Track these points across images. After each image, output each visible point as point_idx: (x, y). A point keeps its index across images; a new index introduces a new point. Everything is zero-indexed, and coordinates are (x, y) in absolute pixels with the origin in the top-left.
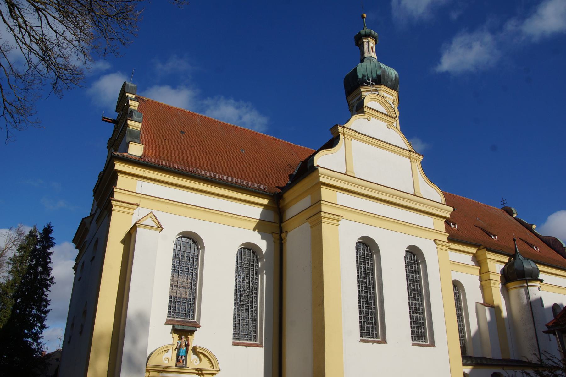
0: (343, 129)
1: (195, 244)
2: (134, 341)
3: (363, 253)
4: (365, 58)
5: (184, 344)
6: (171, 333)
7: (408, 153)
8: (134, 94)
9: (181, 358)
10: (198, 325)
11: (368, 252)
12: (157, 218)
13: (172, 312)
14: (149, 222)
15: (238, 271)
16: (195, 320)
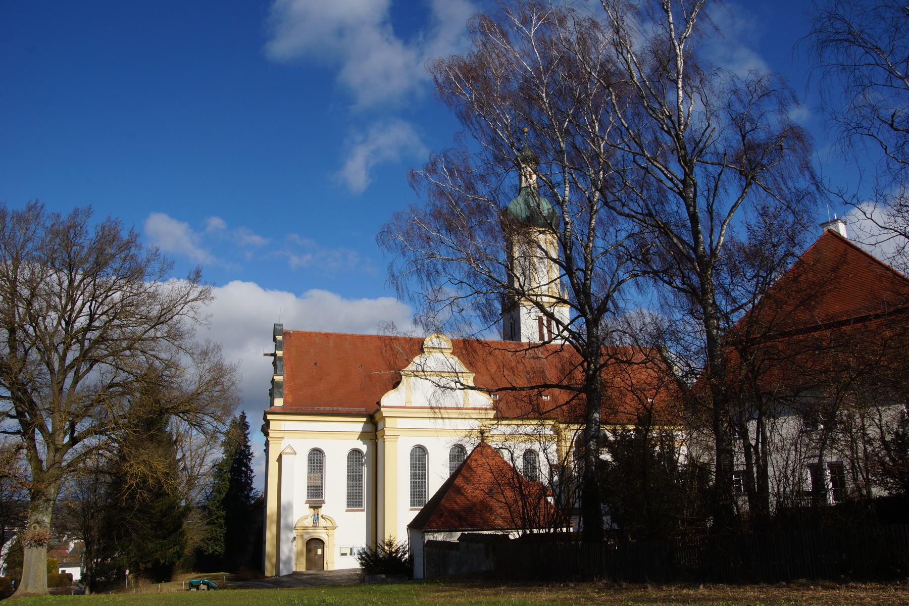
2: (286, 517)
13: (310, 495)
14: (288, 450)
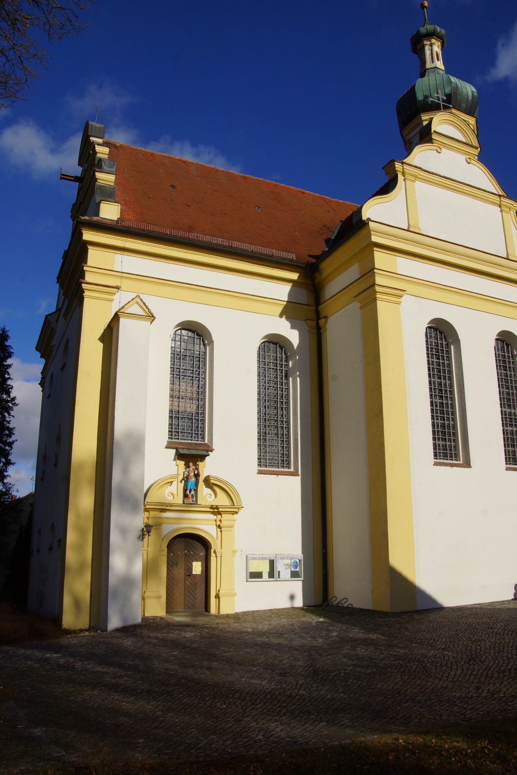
0: (403, 167)
1: (200, 339)
2: (125, 470)
3: (435, 343)
4: (427, 71)
5: (192, 474)
6: (175, 460)
7: (497, 198)
8: (101, 138)
9: (190, 492)
10: (210, 448)
11: (442, 341)
12: (146, 304)
13: (173, 432)
14: (135, 309)
15: (261, 373)
16: (206, 442)
